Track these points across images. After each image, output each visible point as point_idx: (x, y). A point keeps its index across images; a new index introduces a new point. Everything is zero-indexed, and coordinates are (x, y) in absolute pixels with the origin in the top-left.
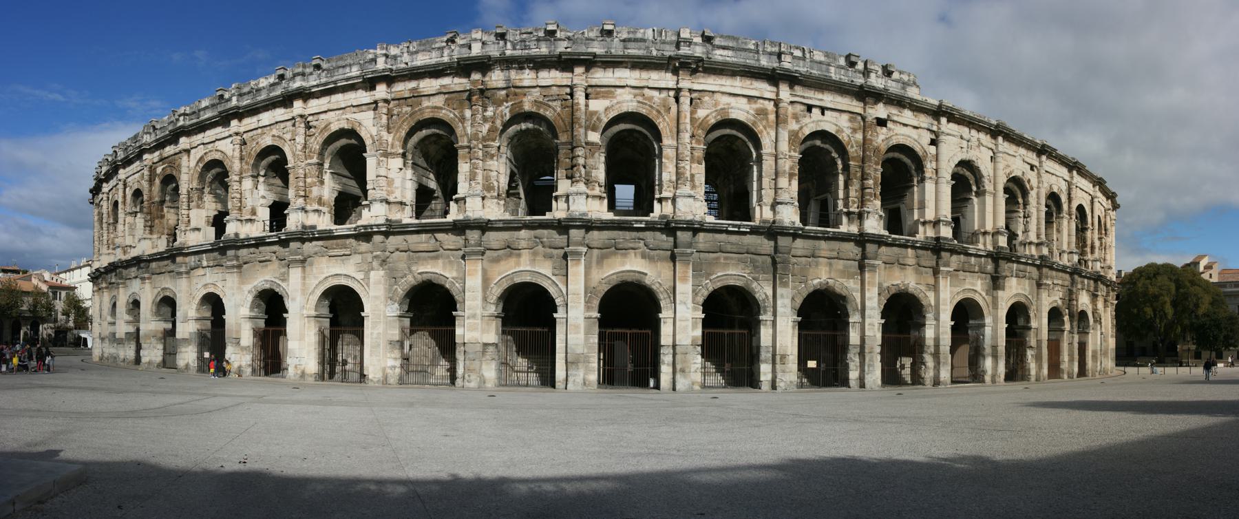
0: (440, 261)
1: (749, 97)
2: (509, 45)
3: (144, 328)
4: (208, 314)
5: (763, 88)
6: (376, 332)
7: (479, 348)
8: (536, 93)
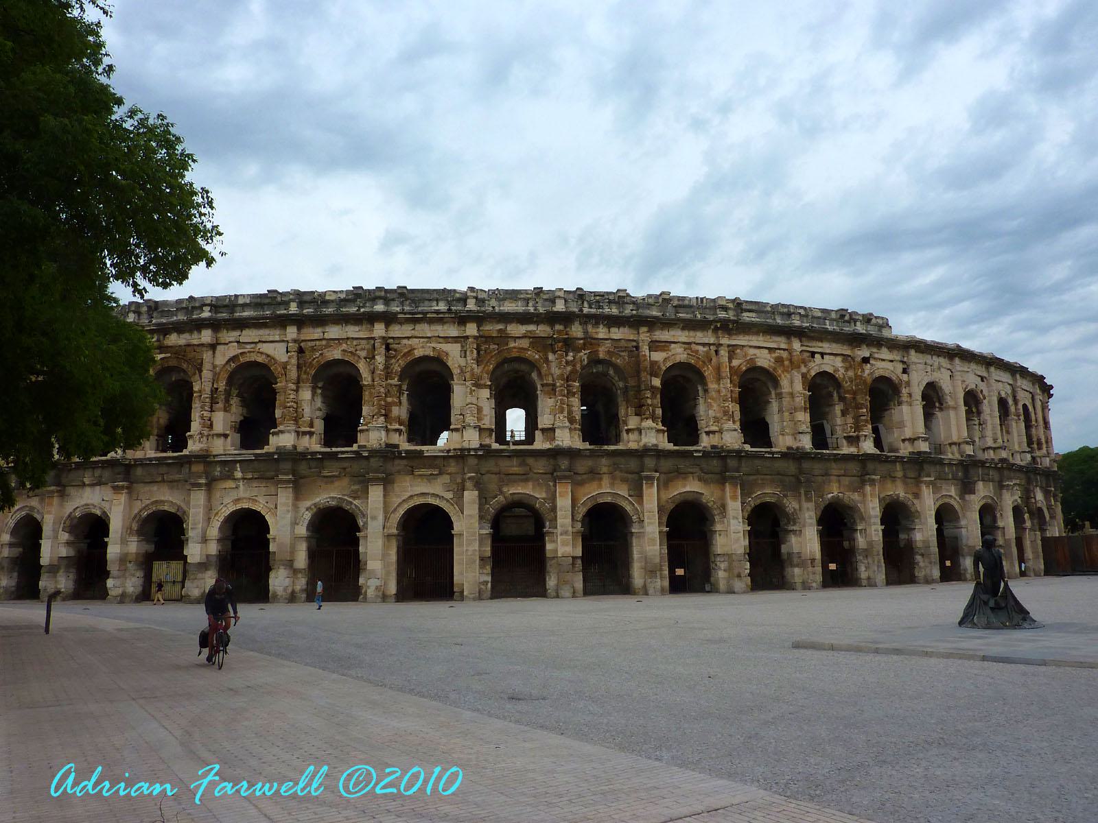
0: (530, 484)
1: (770, 350)
2: (586, 304)
5: (781, 342)
6: (471, 549)
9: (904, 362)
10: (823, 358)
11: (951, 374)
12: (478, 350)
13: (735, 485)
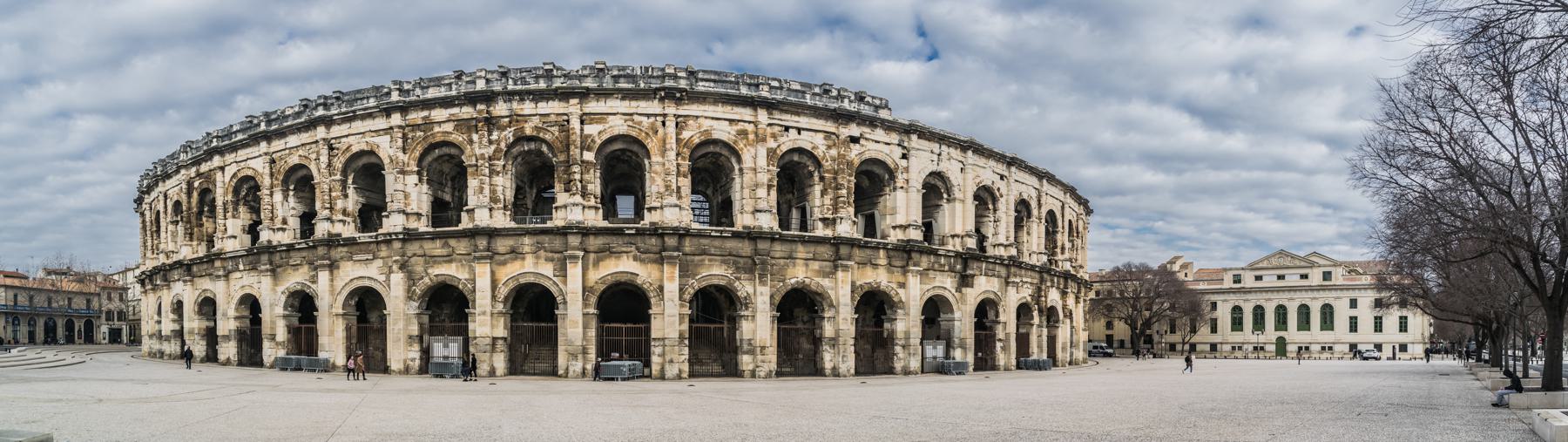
3: (186, 325)
4: (247, 313)
7: (488, 341)
8: (536, 121)
13: (673, 264)
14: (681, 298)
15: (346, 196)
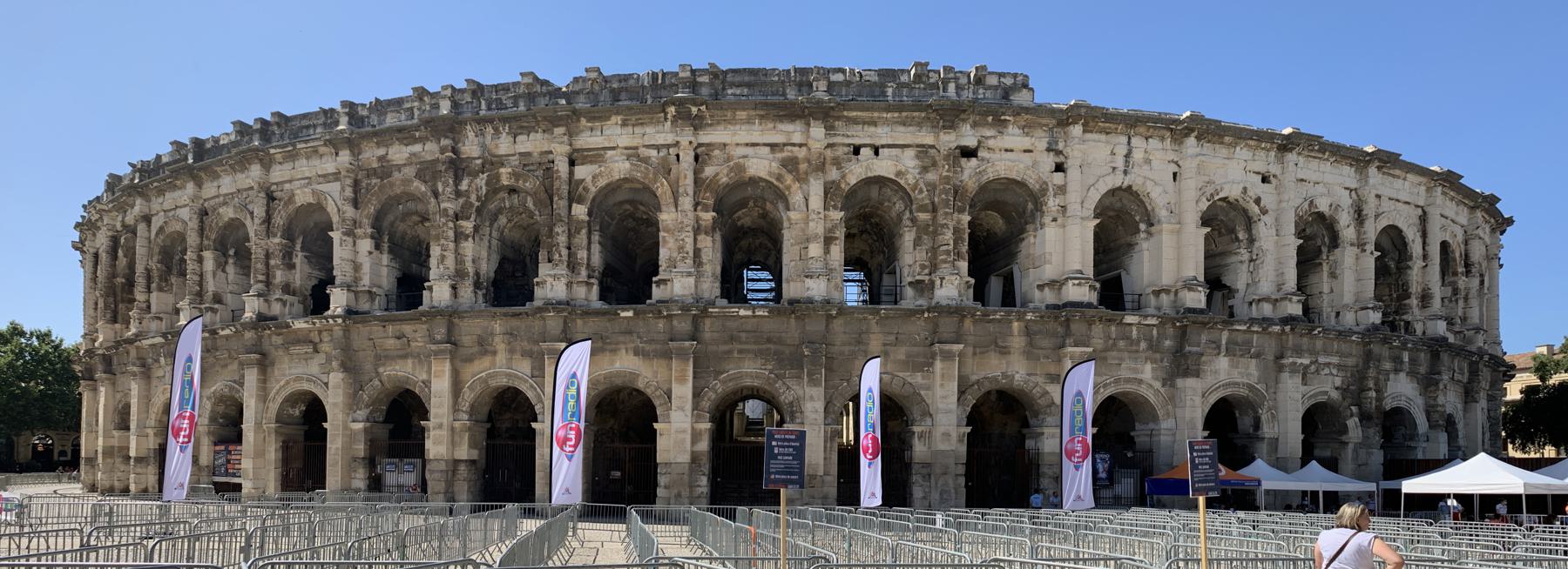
1: (773, 147)
9: (1058, 153)
10: (877, 153)
11: (1176, 169)
12: (356, 184)
14: (696, 407)
15: (292, 267)
